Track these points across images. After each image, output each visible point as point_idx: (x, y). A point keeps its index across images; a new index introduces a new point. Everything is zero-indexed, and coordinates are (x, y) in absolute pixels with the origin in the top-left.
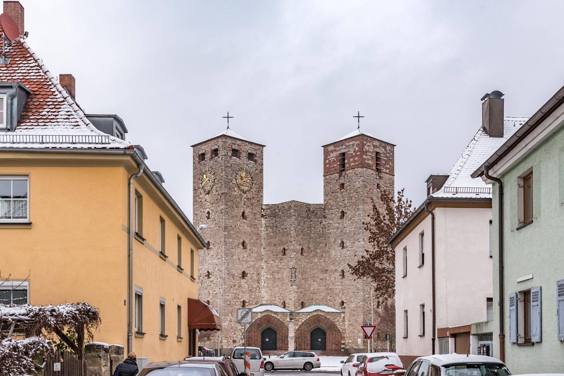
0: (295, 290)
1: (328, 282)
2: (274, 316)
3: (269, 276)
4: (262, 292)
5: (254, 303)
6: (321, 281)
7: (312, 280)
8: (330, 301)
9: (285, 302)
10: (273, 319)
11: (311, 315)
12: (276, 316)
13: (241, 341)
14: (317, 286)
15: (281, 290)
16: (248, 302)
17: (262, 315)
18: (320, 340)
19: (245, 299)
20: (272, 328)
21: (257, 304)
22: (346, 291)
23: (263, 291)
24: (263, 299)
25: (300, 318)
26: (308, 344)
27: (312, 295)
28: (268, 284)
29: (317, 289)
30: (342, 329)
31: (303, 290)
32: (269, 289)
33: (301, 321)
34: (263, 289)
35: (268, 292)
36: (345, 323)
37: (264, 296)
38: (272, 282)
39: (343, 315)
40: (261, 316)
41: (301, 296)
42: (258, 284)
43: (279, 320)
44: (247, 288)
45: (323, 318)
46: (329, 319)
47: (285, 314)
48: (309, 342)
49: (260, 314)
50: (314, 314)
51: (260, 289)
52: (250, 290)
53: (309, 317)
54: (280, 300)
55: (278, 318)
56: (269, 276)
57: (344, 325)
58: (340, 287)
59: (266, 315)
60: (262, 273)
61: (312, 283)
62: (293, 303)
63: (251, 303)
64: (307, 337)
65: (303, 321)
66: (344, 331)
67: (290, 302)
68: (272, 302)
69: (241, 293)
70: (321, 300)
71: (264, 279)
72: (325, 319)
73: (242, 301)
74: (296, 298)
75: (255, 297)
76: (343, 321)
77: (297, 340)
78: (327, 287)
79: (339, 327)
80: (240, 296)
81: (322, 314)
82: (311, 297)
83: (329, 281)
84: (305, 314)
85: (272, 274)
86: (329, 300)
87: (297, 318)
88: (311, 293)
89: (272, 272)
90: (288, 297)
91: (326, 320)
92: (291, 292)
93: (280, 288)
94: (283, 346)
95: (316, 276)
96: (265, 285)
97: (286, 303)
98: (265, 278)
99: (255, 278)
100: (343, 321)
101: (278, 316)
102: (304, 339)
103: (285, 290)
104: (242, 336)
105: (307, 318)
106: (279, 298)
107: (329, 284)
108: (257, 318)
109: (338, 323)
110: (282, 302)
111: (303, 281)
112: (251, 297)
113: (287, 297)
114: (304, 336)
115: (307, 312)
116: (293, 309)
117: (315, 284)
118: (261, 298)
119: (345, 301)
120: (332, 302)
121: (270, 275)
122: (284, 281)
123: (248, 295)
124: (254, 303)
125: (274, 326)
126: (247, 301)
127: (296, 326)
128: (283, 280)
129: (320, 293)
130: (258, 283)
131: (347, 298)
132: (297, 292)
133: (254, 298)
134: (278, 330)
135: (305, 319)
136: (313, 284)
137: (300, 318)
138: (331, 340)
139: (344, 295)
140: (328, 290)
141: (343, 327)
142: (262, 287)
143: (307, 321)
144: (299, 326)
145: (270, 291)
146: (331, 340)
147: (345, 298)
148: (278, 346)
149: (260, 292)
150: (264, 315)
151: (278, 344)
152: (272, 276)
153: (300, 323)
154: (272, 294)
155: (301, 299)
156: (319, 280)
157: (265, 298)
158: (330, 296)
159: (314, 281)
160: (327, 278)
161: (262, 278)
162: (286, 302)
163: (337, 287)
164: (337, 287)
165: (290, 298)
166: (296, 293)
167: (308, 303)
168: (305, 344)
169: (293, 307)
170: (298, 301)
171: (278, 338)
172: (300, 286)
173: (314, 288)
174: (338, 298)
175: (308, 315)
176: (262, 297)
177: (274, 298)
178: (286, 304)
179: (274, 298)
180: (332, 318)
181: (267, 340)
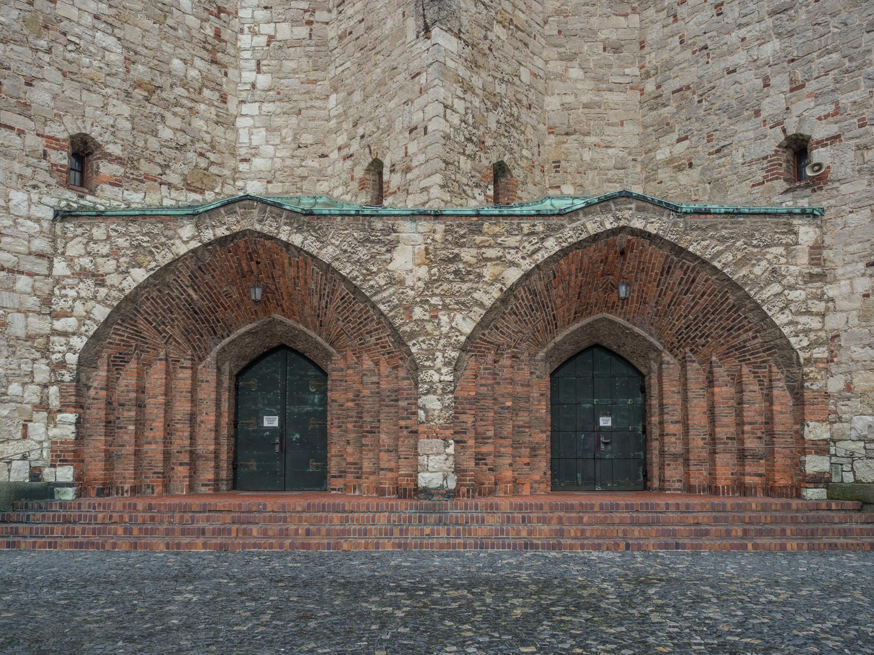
0: (451, 64)
1: (653, 59)
2: (297, 240)
3: (284, 31)
4: (240, 122)
5: (174, 178)
6: (610, 56)
7: (552, 53)
8: (680, 169)
9: (376, 166)
10: (292, 272)
11: (570, 234)
12: (311, 245)
13: (38, 429)
14: (590, 84)
15: (357, 97)
16: (119, 160)
17: (208, 235)
18: (605, 422)
19: (95, 133)
20: (300, 346)
21: (201, 191)
22: (835, 56)
23: (248, 122)
24: (243, 167)
25: (491, 253)
26: (534, 450)
27: (552, 139)
28: (278, 73)
29: (586, 106)
30: (806, 332)
31: (501, 89)
32: (287, 106)
33: (496, 279)
34: (245, 109)
35: (278, 121)
36: (831, 291)
37: (255, 151)
38: (305, 63)
39: (807, 234)
40: (194, 244)
41: (493, 126)
42: (214, 69)
43: (328, 268)
44: (116, 57)
45: (657, 257)
46: (704, 262)
47: (378, 224)
48: (542, 437)
49: (187, 230)
50: (592, 227)
51: (224, 99)
52: (139, 85)
53: (552, 245)
54: (349, 163)
55: (327, 254)
56: (284, 31)
57: (820, 306)
58: (771, 48)
59: (234, 236)
60: (244, 13)
61: (556, 66)
62: (437, 149)
63: (145, 167)
64: (528, 399)
65: (513, 275)
66: (821, 353)
67: (413, 148)
68: (306, 185)
69: (51, 73)
70: (610, 174)
71: (253, 49)
72: (667, 270)
73: (61, 131)
74: (455, 120)
75: (183, 139)
76: (812, 277)
77: (468, 419)
78: (650, 86)
79: (780, 319)
80: (39, 96)
81: (652, 229)
82: (550, 153)
83: (661, 46)
84: (526, 226)
85: (307, 16)
86: (668, 162)
87: (468, 255)
88: (551, 131)
89: (304, 5)
90: (398, 126)
91: (678, 274)
92: (422, 79)
93: (349, 94)
94: (367, 465)
95: (575, 24)
96: (263, 81)
97: (386, 171)
98: (263, 40)
99: (192, 21)
100: (812, 277)
101: (324, 244)
102: (515, 411)
103: (381, 83)
104: (53, 390)
105: (540, 257)
106: (345, 152)
107: (668, 66)
108: (164, 258)
109: (776, 288)
110: (359, 172)
111: (498, 29)
112: (155, 133)
113: (389, 128)
114: (515, 398)
115: (539, 215)
116: (435, 192)
117: (575, 73)
118: (231, 163)
119: (819, 132)
120: (695, 173)
121: (295, 22)
122: (375, 33)
123: (125, 110)
124: (174, 178)
125: (313, 334)
126: (115, 150)
127: (459, 317)
128: (369, 29)
129: (608, 130)
130: (214, 62)
131: (845, 100)
132: (468, 89)
133: (180, 148)
134: (337, 357)
135: (527, 265)
136: (562, 77)
137: (491, 253)
138: (698, 417)
139: (812, 86)
140: (657, 101)
141: (814, 323)
142: (244, 95)
143: (540, 286)
144: (478, 313)
145: (294, 120)
146: (698, 417)
147: (830, 108)
148: (333, 466)
149: (226, 122)
150: (221, 232)
151: (333, 450)
152: (303, 31)
153: (489, 296)
154: (307, 138)
155: (489, 142)
156: (593, 53)
157: (259, 163)
158: (675, 136)
159: (570, 58)
160: (653, 35)
161: (245, 40)
162: (387, 162)
163: (740, 58)
164: (740, 58)
165: (417, 117)
166: (459, 92)
167: (530, 186)
168: (516, 445)
169: (438, 179)
170: (470, 148)
171: (333, 411)
172: (485, 54)
173: (569, 99)
174: (746, 130)
175: (551, 230)
176: (243, 152)
177: (315, 164)
178: (385, 178)
179: (313, 163)
180: (728, 257)
181: (271, 422)
